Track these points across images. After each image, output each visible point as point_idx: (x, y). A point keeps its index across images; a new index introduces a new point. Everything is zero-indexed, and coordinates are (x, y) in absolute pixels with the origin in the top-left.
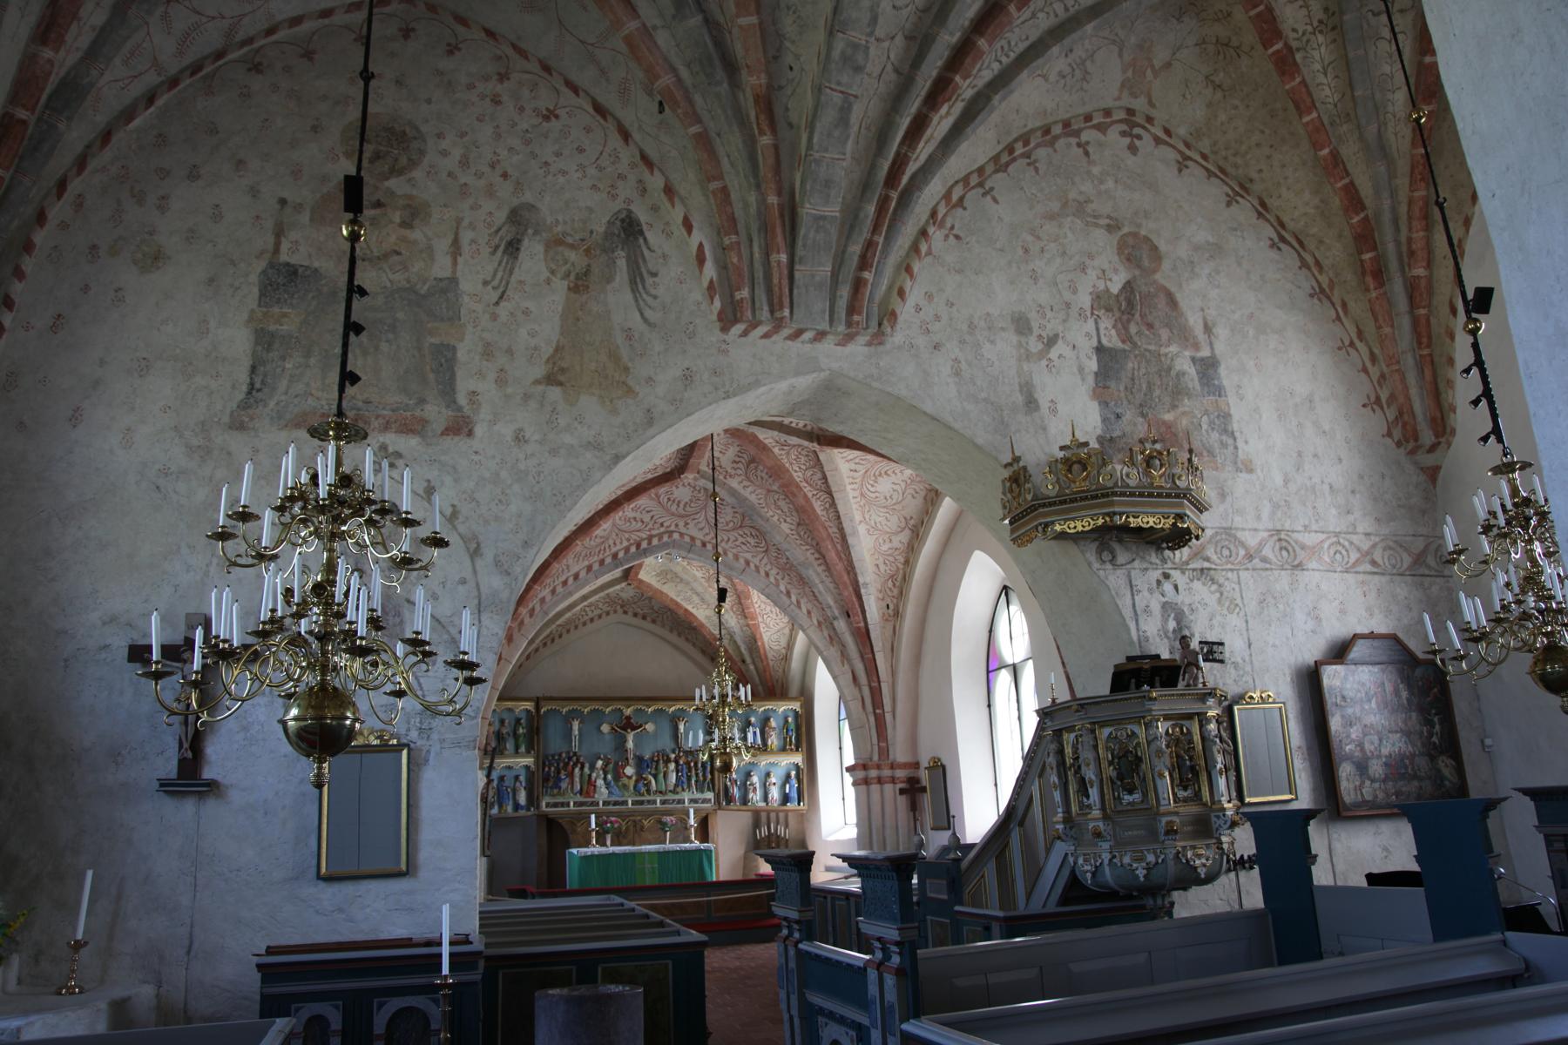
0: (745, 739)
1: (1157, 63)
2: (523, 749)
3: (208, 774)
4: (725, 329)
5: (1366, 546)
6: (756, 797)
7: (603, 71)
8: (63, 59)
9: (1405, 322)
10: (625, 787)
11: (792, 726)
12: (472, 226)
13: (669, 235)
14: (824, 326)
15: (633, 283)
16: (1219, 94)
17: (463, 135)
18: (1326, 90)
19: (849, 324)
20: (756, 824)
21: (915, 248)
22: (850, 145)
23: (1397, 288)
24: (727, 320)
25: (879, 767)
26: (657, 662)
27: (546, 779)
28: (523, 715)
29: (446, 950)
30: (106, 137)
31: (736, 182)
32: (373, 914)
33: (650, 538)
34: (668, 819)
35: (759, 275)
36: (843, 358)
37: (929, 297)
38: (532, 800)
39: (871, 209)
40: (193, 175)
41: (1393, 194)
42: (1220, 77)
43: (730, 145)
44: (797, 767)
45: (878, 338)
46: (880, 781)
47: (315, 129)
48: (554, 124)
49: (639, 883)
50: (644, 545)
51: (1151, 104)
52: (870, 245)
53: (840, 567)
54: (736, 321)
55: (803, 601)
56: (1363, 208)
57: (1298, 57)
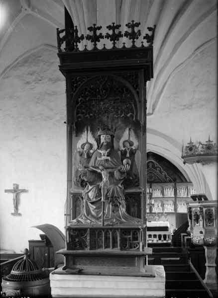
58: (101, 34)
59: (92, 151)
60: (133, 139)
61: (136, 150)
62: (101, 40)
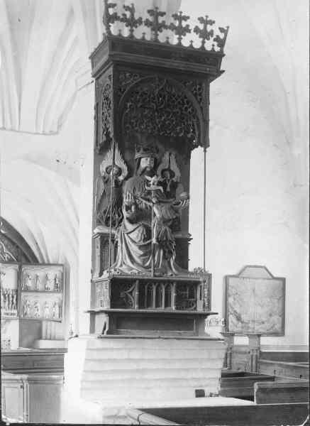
59: (121, 178)
60: (174, 167)
61: (177, 183)
62: (164, 31)
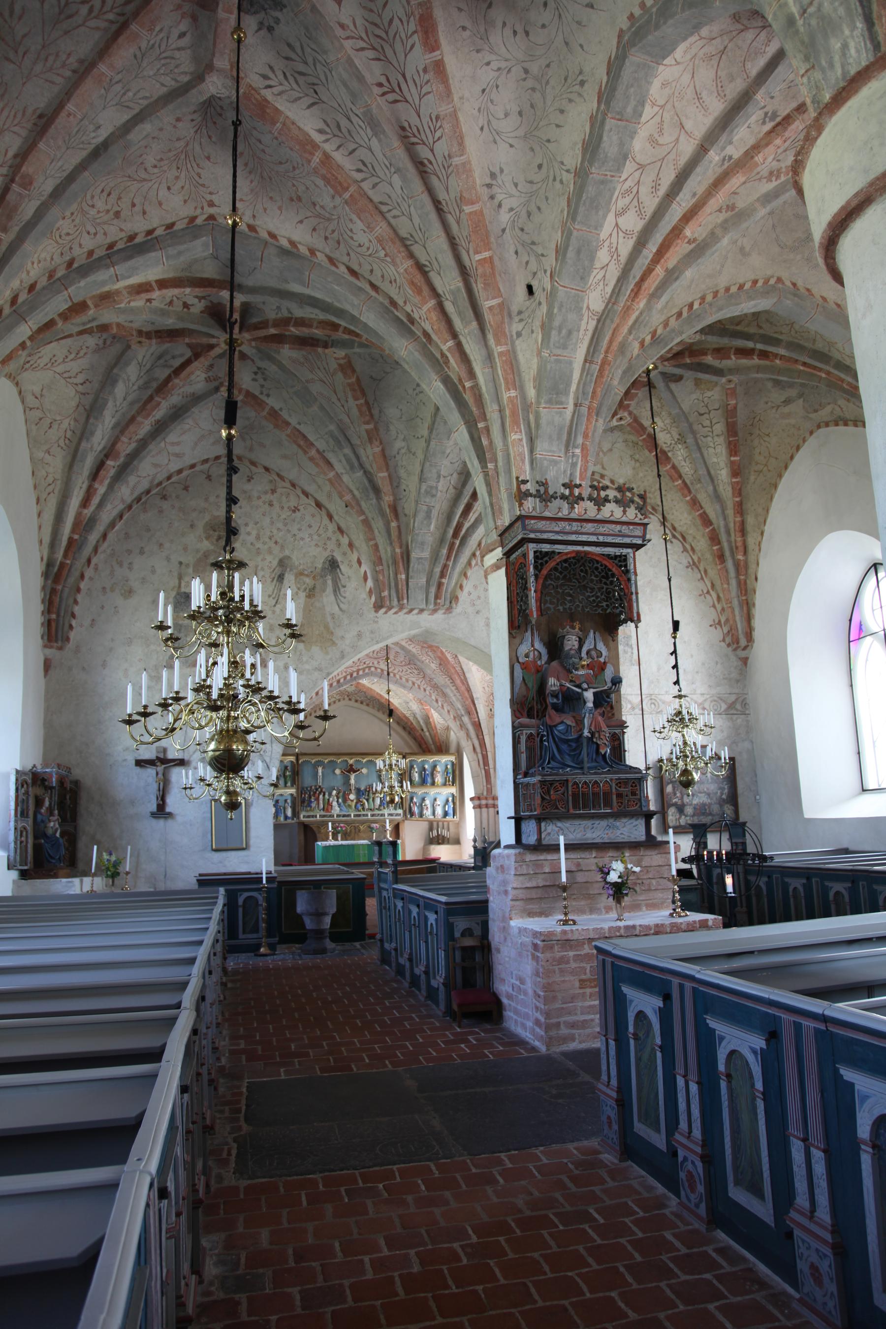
0: (402, 787)
1: (605, 450)
2: (289, 784)
3: (168, 810)
4: (376, 611)
5: (700, 699)
6: (428, 813)
7: (319, 487)
8: (88, 512)
9: (733, 582)
10: (350, 806)
11: (450, 771)
12: (262, 569)
13: (351, 566)
14: (423, 606)
15: (335, 591)
16: (638, 464)
17: (256, 523)
18: (686, 469)
19: (435, 604)
20: (431, 829)
21: (469, 564)
22: (432, 527)
23: (730, 564)
24: (378, 607)
25: (486, 799)
26: (368, 729)
27: (303, 802)
28: (289, 765)
29: (264, 876)
30: (104, 536)
31: (381, 541)
32: (234, 863)
33: (358, 671)
34: (374, 825)
35: (393, 584)
36: (431, 621)
37: (475, 587)
38: (295, 814)
39: (445, 551)
40: (142, 552)
41: (725, 519)
42: (637, 457)
43: (378, 525)
44: (453, 796)
45: (449, 610)
46: (487, 806)
47: (192, 526)
48: (298, 514)
49: (357, 861)
50: (355, 675)
51: (603, 468)
52: (445, 566)
53: (463, 688)
54: (381, 607)
55: (445, 705)
56: (711, 524)
57: (670, 454)
58: (580, 494)
60: (601, 646)
61: (605, 663)
62: (581, 503)
